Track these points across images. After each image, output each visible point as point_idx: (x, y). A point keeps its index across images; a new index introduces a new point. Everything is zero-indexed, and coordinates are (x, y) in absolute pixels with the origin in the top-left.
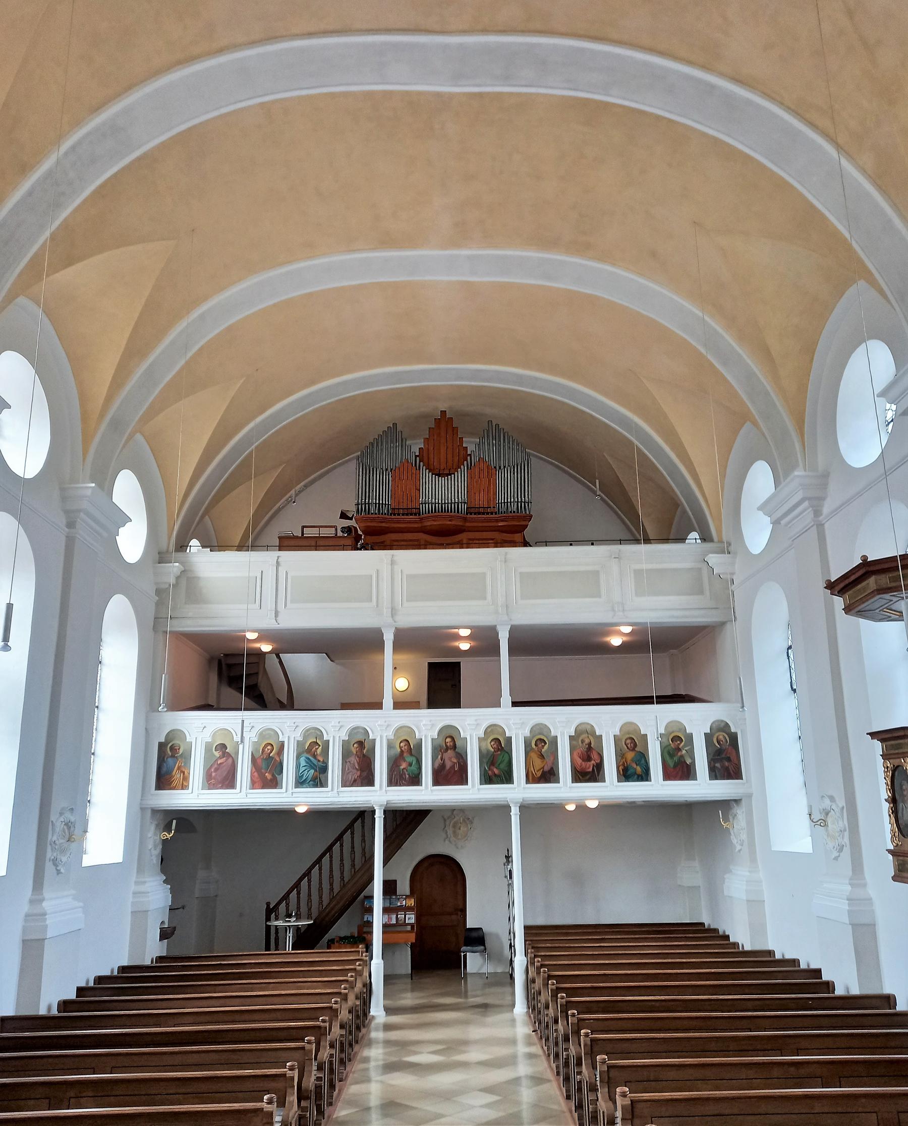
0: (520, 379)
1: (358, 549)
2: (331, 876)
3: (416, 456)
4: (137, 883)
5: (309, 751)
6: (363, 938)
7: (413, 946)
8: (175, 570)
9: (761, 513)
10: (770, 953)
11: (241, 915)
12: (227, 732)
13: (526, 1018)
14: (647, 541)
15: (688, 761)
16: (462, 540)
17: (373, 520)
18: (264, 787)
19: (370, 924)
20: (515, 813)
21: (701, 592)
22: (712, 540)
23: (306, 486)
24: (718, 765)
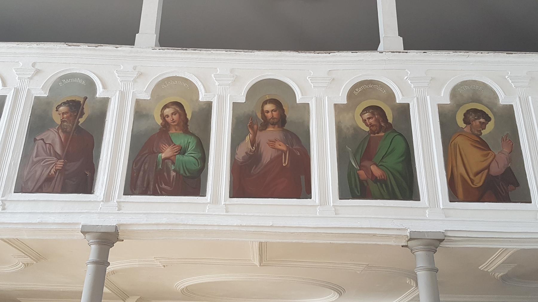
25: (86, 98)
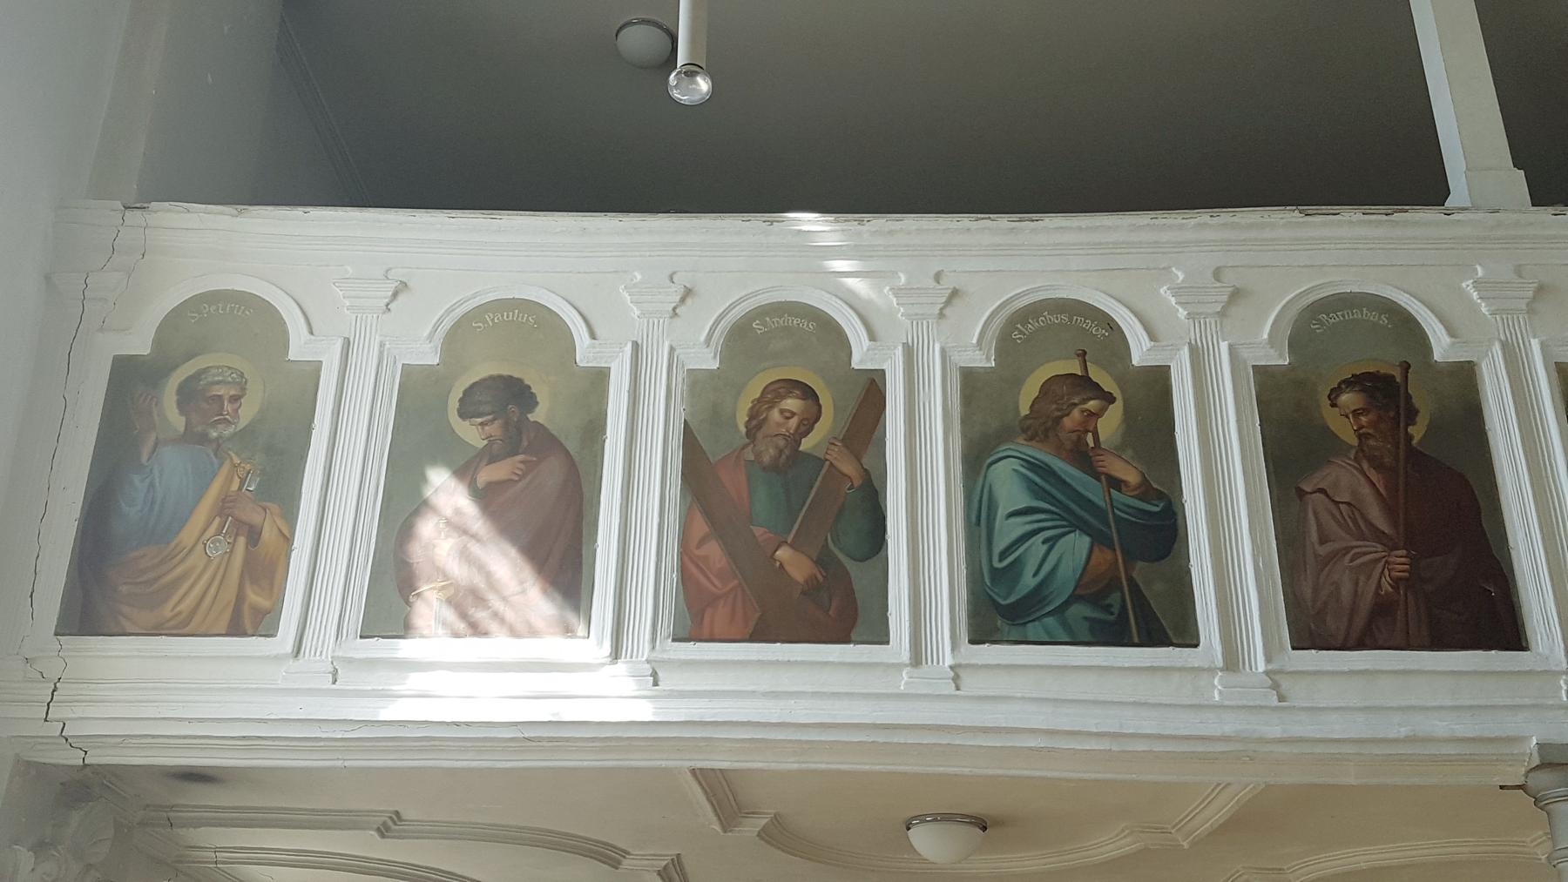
5: (1041, 425)
12: (535, 325)
18: (765, 629)
25: (1406, 367)
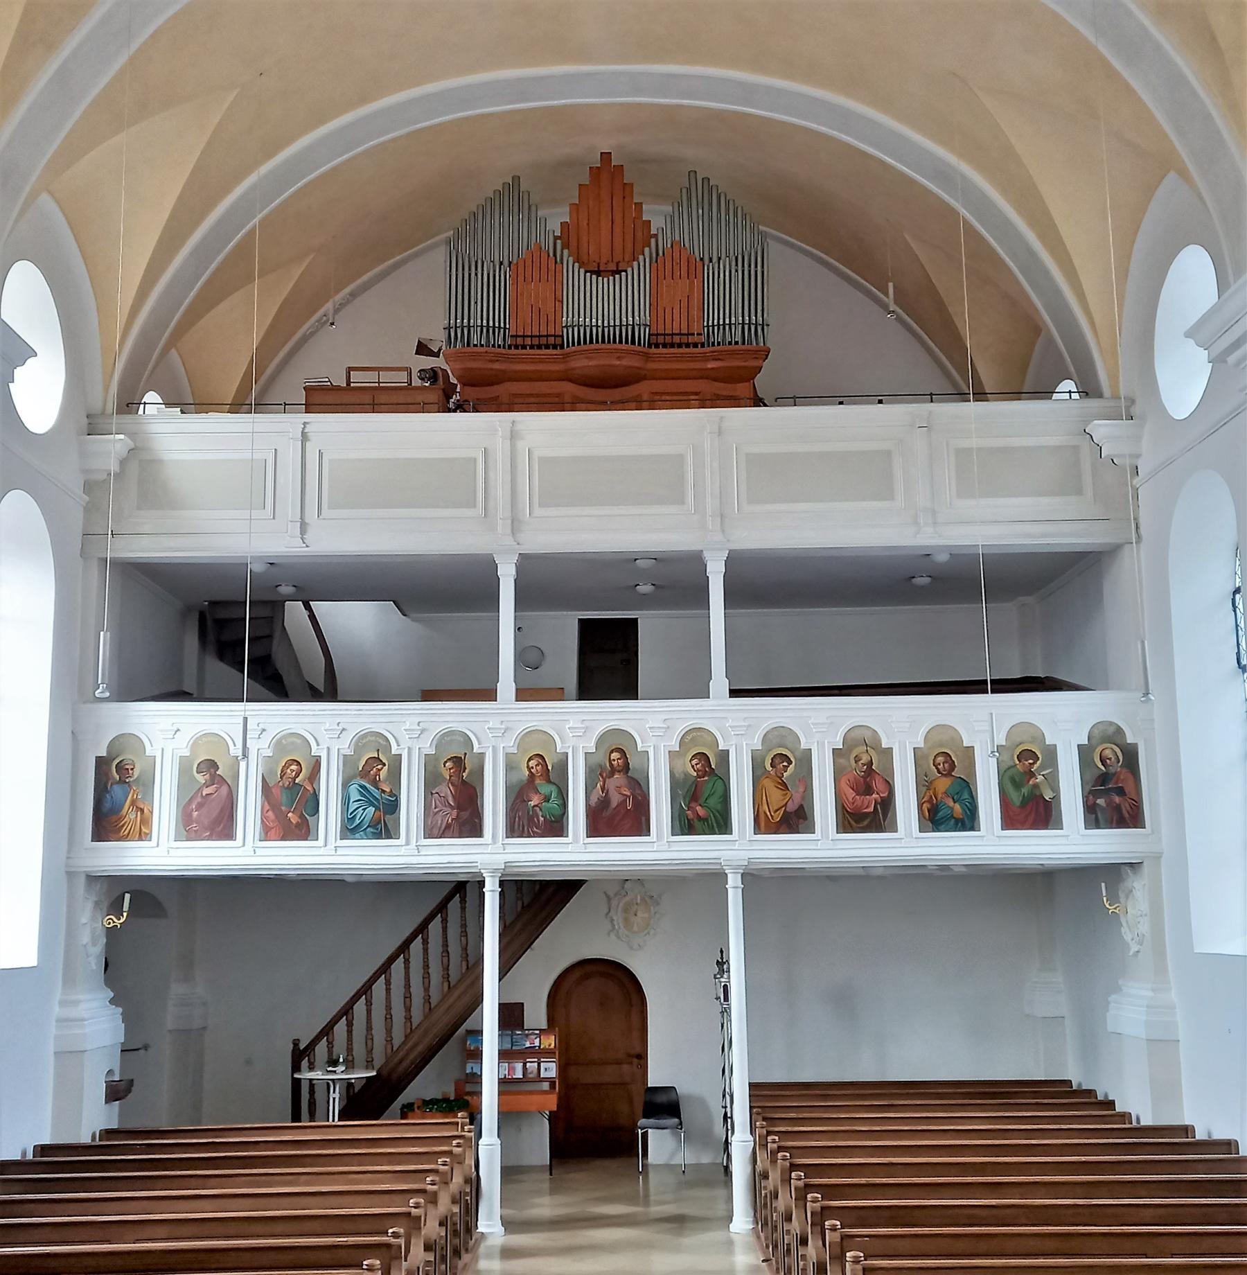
0: (749, 92)
1: (449, 411)
2: (408, 996)
3: (556, 238)
4: (63, 1003)
5: (364, 773)
6: (463, 1101)
7: (553, 1118)
8: (118, 446)
9: (1191, 341)
10: (1187, 1130)
11: (248, 1062)
12: (216, 739)
13: (752, 1239)
14: (981, 395)
15: (1048, 796)
16: (640, 395)
17: (474, 356)
19: (476, 1079)
20: (734, 882)
21: (1079, 491)
22: (1100, 395)
23: (353, 295)
24: (1101, 802)
